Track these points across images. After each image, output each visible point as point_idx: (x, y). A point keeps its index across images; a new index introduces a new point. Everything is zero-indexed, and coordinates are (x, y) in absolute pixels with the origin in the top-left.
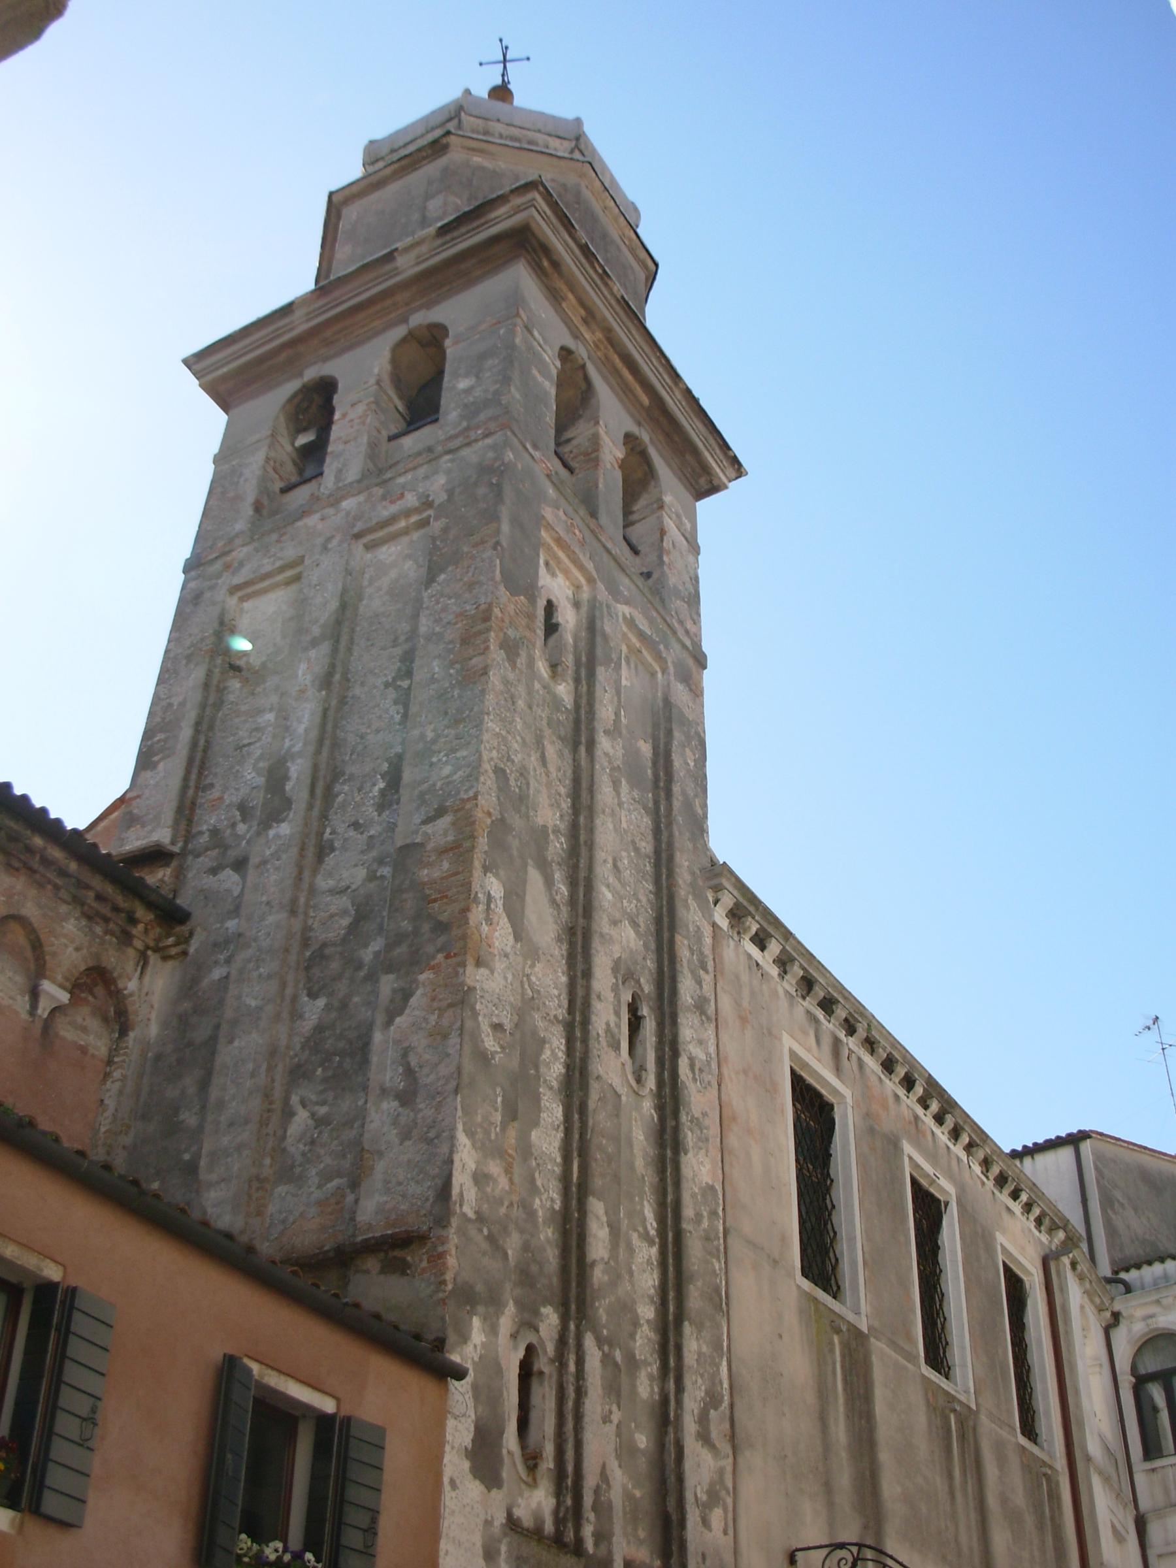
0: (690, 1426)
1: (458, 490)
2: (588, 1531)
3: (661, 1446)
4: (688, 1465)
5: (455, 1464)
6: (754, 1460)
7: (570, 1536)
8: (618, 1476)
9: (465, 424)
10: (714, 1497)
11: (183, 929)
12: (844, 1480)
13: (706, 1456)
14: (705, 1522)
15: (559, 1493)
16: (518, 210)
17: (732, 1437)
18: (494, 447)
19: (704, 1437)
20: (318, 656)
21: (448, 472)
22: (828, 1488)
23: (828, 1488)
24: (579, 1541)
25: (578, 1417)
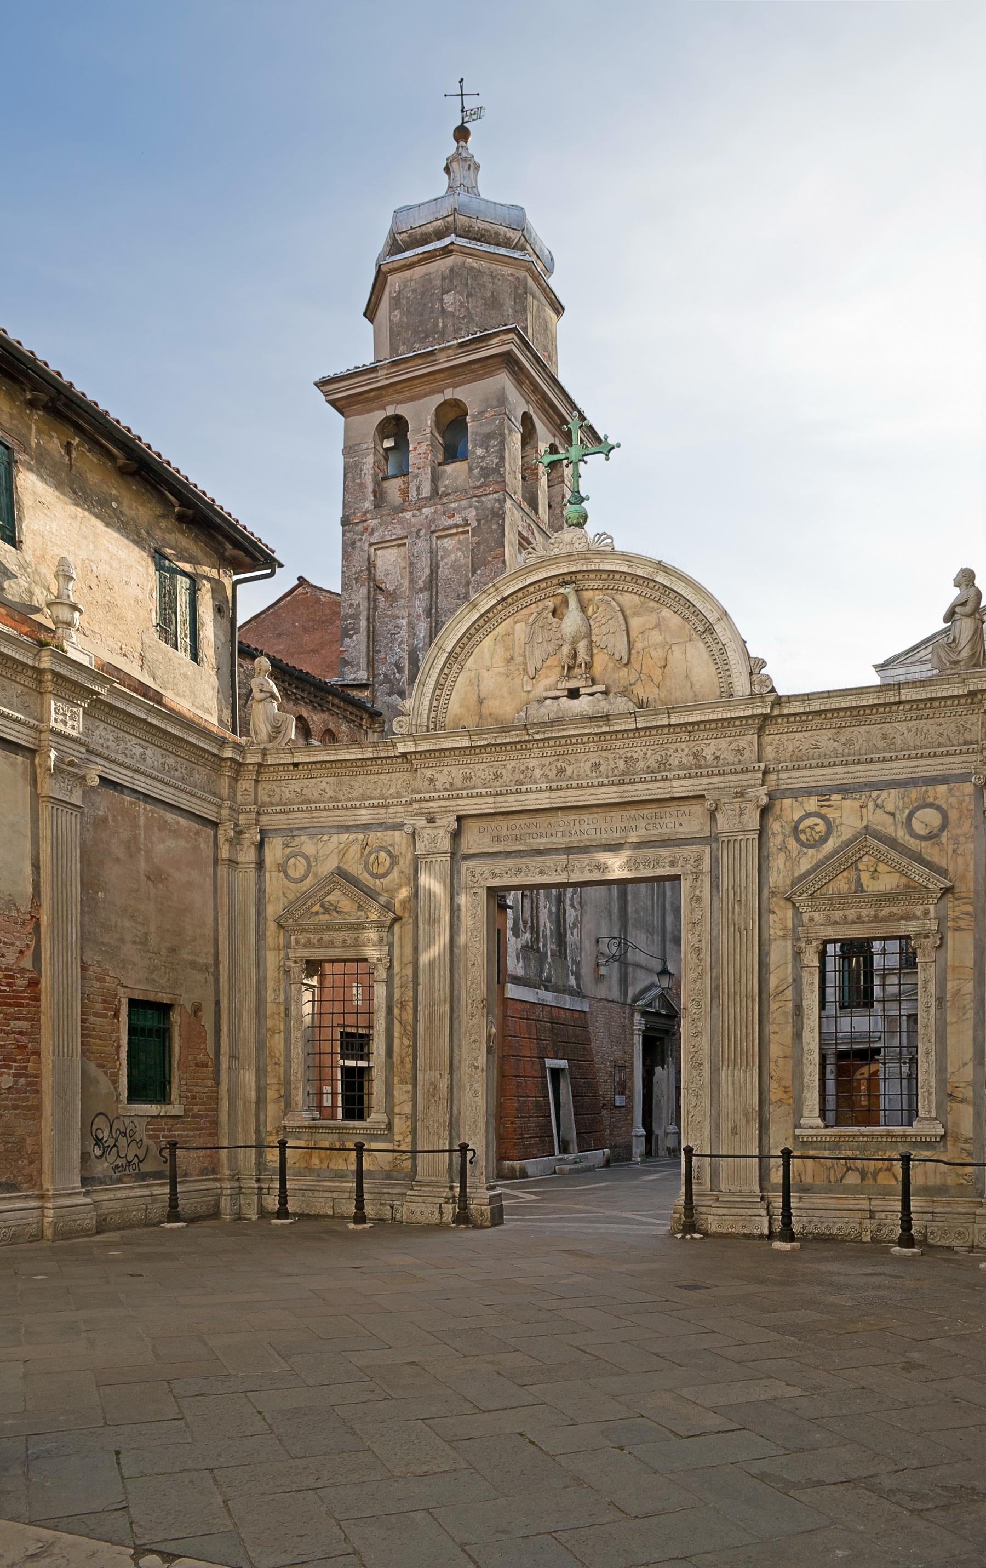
0: (568, 902)
1: (483, 522)
2: (541, 945)
3: (558, 910)
4: (567, 915)
5: (509, 933)
6: (589, 909)
7: (535, 947)
8: (548, 925)
9: (483, 480)
10: (575, 925)
11: (381, 719)
12: (615, 910)
13: (573, 911)
14: (572, 934)
15: (532, 934)
16: (503, 343)
17: (580, 903)
18: (498, 500)
19: (572, 905)
20: (424, 596)
21: (477, 508)
22: (610, 913)
23: (610, 913)
24: (538, 948)
25: (537, 908)
